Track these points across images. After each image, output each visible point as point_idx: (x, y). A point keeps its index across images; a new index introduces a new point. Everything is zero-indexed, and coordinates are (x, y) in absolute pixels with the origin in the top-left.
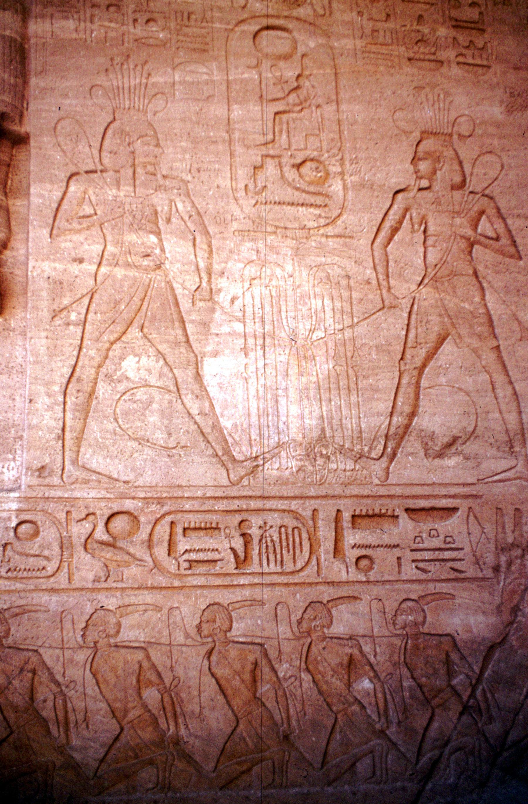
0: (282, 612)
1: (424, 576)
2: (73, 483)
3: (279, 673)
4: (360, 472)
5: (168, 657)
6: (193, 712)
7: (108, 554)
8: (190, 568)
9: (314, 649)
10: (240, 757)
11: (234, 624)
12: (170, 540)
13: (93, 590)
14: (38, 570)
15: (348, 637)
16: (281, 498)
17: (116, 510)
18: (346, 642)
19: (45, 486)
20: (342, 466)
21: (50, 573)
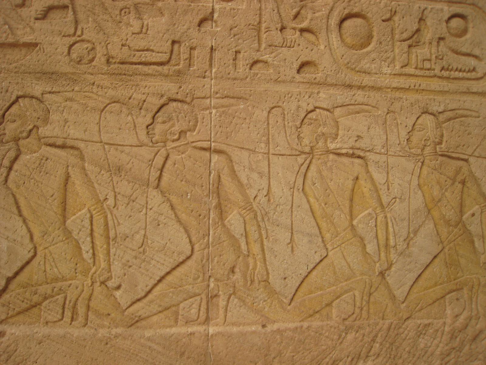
21: (479, 75)
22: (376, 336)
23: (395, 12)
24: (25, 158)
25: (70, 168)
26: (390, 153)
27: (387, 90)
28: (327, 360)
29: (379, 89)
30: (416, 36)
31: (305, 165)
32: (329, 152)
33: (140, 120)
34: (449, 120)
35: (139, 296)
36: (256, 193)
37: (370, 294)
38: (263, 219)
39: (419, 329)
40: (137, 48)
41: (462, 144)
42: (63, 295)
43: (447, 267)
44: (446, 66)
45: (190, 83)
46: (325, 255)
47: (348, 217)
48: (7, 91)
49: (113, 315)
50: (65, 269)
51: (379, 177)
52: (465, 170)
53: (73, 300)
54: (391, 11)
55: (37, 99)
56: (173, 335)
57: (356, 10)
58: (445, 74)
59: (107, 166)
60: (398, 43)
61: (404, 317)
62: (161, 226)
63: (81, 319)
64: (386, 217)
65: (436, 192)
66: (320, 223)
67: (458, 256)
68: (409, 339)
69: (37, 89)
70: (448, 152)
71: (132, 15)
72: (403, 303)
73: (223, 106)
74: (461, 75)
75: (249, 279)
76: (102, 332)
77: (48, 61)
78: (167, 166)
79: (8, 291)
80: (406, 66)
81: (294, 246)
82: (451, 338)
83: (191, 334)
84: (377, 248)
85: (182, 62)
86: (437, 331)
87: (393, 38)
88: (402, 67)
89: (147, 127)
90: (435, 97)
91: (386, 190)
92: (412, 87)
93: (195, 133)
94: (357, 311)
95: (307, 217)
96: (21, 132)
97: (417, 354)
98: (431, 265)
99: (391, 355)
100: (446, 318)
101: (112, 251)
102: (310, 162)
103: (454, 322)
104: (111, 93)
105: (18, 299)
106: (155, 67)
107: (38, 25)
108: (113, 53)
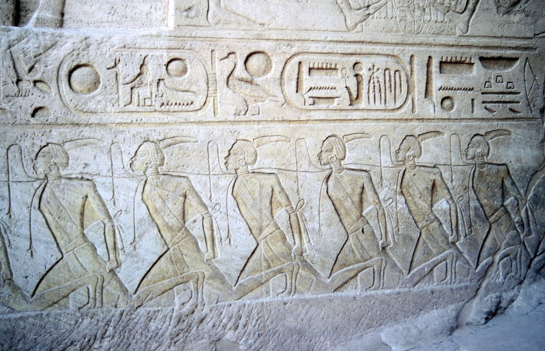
0: (384, 143)
1: (490, 116)
2: (217, 24)
3: (380, 196)
4: (447, 24)
5: (295, 182)
6: (314, 229)
7: (247, 89)
8: (314, 103)
9: (407, 175)
10: (349, 265)
11: (348, 153)
12: (298, 78)
13: (233, 122)
15: (432, 165)
16: (387, 44)
17: (253, 50)
18: (431, 169)
19: (192, 26)
20: (434, 18)
22: (110, 321)
23: (119, 60)
26: (114, 175)
27: (112, 125)
31: (41, 189)
38: (6, 232)
39: (150, 314)
41: (182, 165)
43: (173, 264)
46: (61, 257)
47: (79, 228)
51: (106, 195)
61: (136, 306)
67: (182, 255)
70: (169, 171)
72: (134, 294)
81: (33, 251)
82: (179, 322)
84: (106, 250)
86: (166, 316)
91: (113, 205)
92: (134, 121)
95: (43, 229)
97: (149, 336)
98: (158, 263)
99: (124, 336)
100: (174, 306)
102: (45, 186)
103: (181, 309)
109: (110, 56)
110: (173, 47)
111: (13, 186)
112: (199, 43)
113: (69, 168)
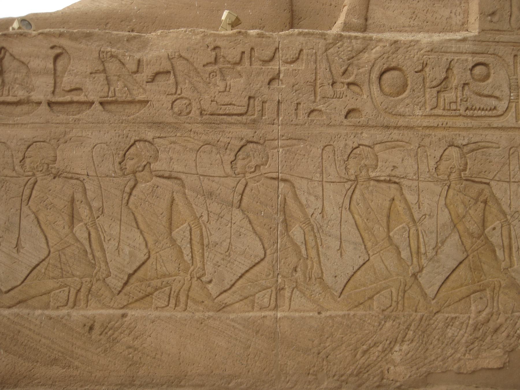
14: (490, 110)
19: (495, 30)
21: (499, 113)
22: (410, 325)
23: (427, 64)
24: (141, 186)
25: (174, 193)
26: (420, 179)
27: (419, 129)
28: (370, 342)
29: (412, 128)
30: (444, 83)
32: (370, 179)
33: (226, 157)
34: (473, 150)
35: (226, 288)
36: (313, 211)
37: (405, 291)
39: (448, 321)
40: (223, 103)
41: (484, 171)
42: (169, 287)
43: (471, 271)
44: (470, 107)
45: (262, 129)
46: (367, 259)
47: (386, 230)
48: (127, 137)
49: (206, 302)
50: (171, 268)
51: (411, 198)
52: (487, 192)
53: (177, 291)
54: (423, 63)
55: (149, 142)
56: (250, 317)
57: (393, 65)
58: (469, 113)
59: (202, 192)
60: (429, 90)
61: (434, 311)
62: (242, 236)
63: (182, 305)
64: (417, 230)
65: (461, 210)
66: (363, 234)
67: (481, 262)
68: (439, 329)
69: (150, 135)
70: (471, 177)
71: (218, 77)
72: (433, 299)
73: (288, 146)
74: (483, 113)
75: (307, 276)
76: (198, 315)
77: (157, 114)
78: (246, 191)
79: (129, 284)
80: (435, 108)
81: (343, 251)
82: (475, 330)
83: (264, 317)
84: (410, 254)
85: (256, 113)
86: (463, 323)
87: (424, 86)
88: (432, 109)
89: (231, 163)
90: (460, 133)
91: (417, 209)
92: (440, 125)
93: (266, 167)
94: (394, 304)
95: (352, 230)
96: (138, 167)
97: (446, 342)
98: (457, 269)
99: (423, 341)
100: (471, 313)
101: (206, 254)
102: (355, 187)
104: (204, 137)
105: (136, 290)
106: (236, 117)
107: (148, 86)
108: (205, 107)
109: (418, 60)
110: (477, 52)
111: (327, 186)
112: (502, 47)
113: (378, 169)
